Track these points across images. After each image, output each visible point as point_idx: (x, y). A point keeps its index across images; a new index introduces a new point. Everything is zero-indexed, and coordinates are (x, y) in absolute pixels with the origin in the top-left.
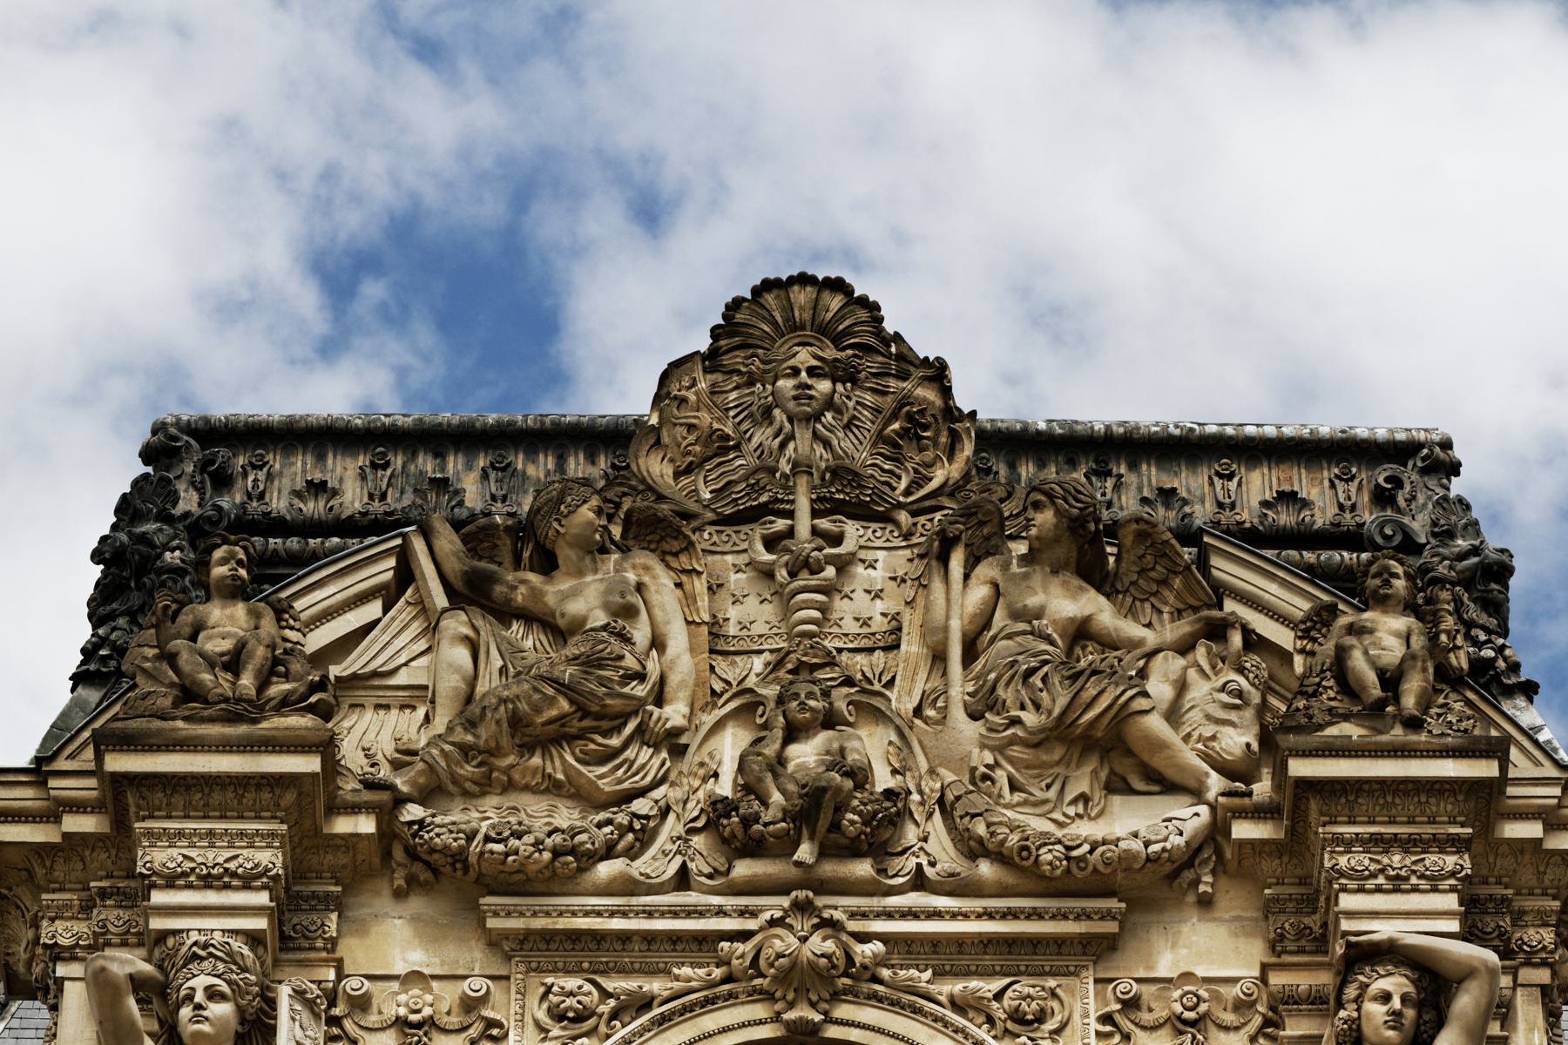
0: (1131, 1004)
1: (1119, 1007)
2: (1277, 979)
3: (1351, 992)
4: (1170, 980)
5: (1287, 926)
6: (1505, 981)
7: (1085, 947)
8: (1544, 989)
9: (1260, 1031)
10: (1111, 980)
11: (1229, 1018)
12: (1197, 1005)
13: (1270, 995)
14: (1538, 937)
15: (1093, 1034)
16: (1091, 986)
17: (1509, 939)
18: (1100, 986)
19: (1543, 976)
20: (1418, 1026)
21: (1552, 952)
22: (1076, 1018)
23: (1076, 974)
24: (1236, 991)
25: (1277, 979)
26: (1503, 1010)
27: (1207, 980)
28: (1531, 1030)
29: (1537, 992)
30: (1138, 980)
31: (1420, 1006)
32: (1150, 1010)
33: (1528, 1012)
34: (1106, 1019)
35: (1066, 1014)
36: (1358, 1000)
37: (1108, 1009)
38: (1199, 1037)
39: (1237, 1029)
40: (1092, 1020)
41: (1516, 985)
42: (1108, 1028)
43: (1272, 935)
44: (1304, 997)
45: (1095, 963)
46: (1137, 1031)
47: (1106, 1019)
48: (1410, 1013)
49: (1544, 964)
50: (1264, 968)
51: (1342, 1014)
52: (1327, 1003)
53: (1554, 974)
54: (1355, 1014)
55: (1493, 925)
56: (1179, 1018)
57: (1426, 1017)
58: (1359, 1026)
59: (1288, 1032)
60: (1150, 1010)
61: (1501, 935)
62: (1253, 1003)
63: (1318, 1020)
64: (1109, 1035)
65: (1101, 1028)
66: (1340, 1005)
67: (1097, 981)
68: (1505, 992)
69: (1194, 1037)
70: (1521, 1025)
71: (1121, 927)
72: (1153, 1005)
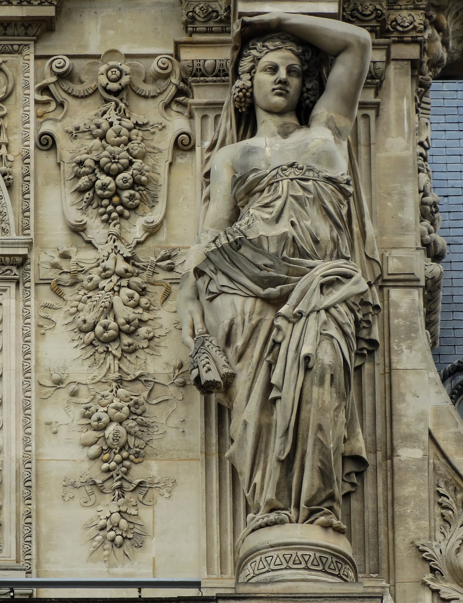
0: (65, 76)
1: (54, 79)
2: (188, 55)
3: (246, 64)
4: (98, 57)
5: (197, 10)
6: (380, 56)
7: (26, 28)
8: (415, 65)
9: (173, 100)
10: (48, 57)
11: (148, 89)
12: (120, 77)
13: (183, 69)
14: (410, 18)
15: (32, 103)
16: (32, 62)
17: (384, 20)
18: (39, 62)
19: (413, 52)
20: (302, 93)
21: (420, 32)
22: (19, 89)
23: (19, 52)
24: (153, 66)
25: (188, 55)
26: (376, 80)
27: (128, 56)
28: (402, 98)
29: (408, 66)
30: (70, 57)
31: (304, 76)
32: (82, 82)
33: (399, 84)
34: (44, 89)
35: (10, 86)
36: (252, 71)
37: (45, 82)
38: (122, 105)
39: (154, 97)
40: (32, 91)
41: (388, 61)
42: (45, 98)
43: (184, 18)
44: (210, 70)
45: (36, 42)
46: (70, 100)
47: (44, 89)
48: (295, 82)
49: (414, 41)
50: (177, 45)
51: (238, 83)
52: (227, 75)
53: (423, 51)
54: (249, 84)
55: (371, 8)
56: (105, 89)
57: (309, 86)
58: (252, 93)
59: (196, 100)
60: (82, 82)
61: (378, 17)
62: (167, 77)
63: (222, 90)
64: (46, 103)
65: (39, 98)
66: (236, 76)
67: (37, 58)
68: (379, 65)
69: (117, 105)
70: (393, 94)
71: (56, 12)
72: (83, 78)
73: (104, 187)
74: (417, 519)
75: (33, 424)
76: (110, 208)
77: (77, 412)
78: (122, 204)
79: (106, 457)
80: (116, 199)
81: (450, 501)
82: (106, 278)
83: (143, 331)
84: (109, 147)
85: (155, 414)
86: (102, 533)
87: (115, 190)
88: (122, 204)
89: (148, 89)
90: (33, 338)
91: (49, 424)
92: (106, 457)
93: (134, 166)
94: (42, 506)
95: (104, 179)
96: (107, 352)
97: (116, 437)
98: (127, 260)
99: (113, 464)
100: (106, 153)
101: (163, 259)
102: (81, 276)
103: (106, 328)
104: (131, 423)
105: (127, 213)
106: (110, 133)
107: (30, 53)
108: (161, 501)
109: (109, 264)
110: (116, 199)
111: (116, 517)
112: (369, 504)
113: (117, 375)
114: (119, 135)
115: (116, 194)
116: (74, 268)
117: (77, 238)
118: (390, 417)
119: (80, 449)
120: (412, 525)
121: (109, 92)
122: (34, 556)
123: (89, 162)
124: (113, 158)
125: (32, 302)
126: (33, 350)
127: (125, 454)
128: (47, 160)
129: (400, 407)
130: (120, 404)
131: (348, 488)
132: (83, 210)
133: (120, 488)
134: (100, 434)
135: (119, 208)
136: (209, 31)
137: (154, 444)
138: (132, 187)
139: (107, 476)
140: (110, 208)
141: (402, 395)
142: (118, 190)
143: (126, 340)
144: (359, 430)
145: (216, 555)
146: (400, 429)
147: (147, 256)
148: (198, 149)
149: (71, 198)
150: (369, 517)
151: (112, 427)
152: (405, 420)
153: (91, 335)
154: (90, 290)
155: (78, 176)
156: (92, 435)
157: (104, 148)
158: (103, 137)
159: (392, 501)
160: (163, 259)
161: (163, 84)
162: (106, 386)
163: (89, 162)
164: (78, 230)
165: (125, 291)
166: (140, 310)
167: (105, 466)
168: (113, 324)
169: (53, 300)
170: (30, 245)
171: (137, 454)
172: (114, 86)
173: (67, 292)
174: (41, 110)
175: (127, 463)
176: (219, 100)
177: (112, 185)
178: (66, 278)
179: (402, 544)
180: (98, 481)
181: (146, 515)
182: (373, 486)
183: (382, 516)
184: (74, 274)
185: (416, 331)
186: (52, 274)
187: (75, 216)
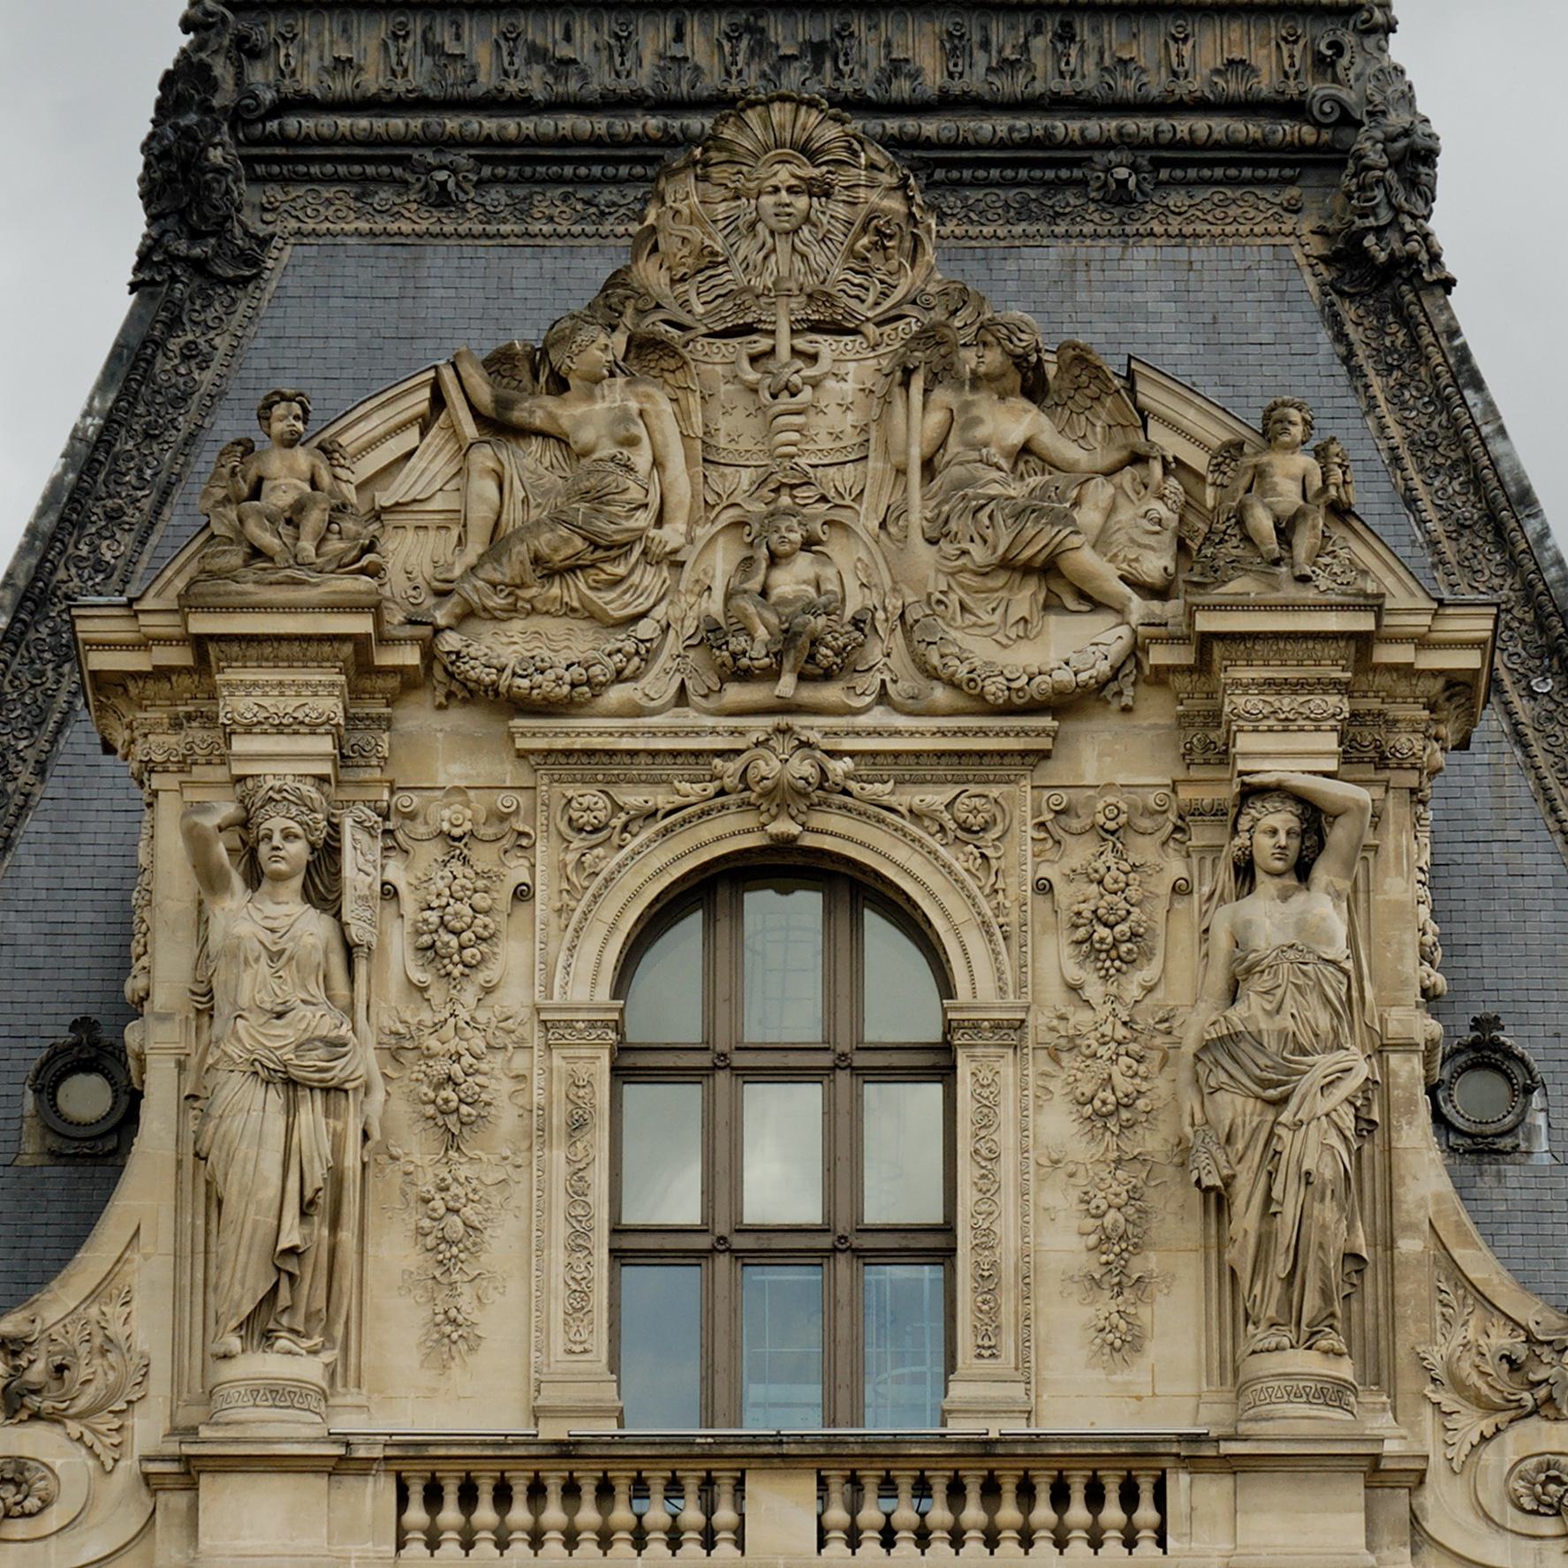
1: (1051, 816)
2: (1185, 794)
40: (1029, 828)
42: (1043, 835)
43: (1182, 750)
46: (1067, 837)
47: (1041, 825)
59: (1193, 842)
73: (1102, 941)
74: (1418, 1321)
75: (1032, 1212)
76: (1108, 963)
77: (1075, 1195)
78: (1119, 958)
79: (1104, 1248)
80: (1113, 954)
81: (1450, 1299)
82: (1105, 1044)
83: (1141, 1104)
84: (1108, 897)
85: (1153, 1198)
86: (1102, 1335)
87: (1112, 945)
88: (1119, 958)
89: (1146, 823)
90: (1030, 1112)
91: (1046, 1209)
92: (1104, 1248)
93: (1132, 917)
94: (1041, 1303)
95: (1102, 932)
96: (1105, 1126)
97: (1115, 1227)
98: (1125, 1024)
99: (1112, 1257)
100: (1103, 903)
101: (1161, 1021)
102: (1078, 1041)
103: (1104, 1103)
104: (1130, 1210)
105: (1124, 967)
106: (1108, 880)
107: (1026, 784)
108: (1159, 1298)
109: (1107, 1029)
110: (1113, 954)
111: (1115, 1318)
112: (1369, 1306)
113: (1116, 1154)
114: (1116, 882)
115: (1115, 946)
116: (1071, 1032)
117: (1073, 995)
118: (1390, 1201)
119: (1076, 1238)
120: (1412, 1328)
121: (1107, 831)
122: (1033, 1364)
123: (1087, 914)
124: (1111, 909)
125: (1030, 1072)
126: (1031, 1127)
127: (1124, 1245)
128: (1043, 904)
129: (1399, 1191)
130: (1118, 1190)
132: (1081, 965)
133: (1119, 1283)
134: (1099, 1222)
135: (1117, 963)
136: (1207, 763)
137: (1153, 1233)
138: (1129, 940)
139: (1104, 1269)
140: (1108, 963)
141: (1402, 1177)
142: (1116, 944)
143: (1125, 1115)
145: (1216, 1364)
146: (1400, 1217)
147: (1145, 1020)
148: (1196, 896)
149: (1068, 950)
150: (1369, 1321)
151: (1112, 1213)
152: (1405, 1207)
153: (1088, 1110)
154: (1088, 1057)
155: (1076, 926)
156: (1091, 1223)
157: (1102, 896)
158: (1100, 882)
159: (1392, 1300)
160: (1161, 1021)
161: (1160, 819)
162: (1102, 1166)
163: (1087, 914)
164: (1074, 989)
165: (1124, 1060)
166: (1137, 1081)
167: (1104, 1258)
168: (1112, 1099)
169: (1049, 1067)
170: (1028, 1008)
172: (1111, 825)
173: (1064, 1057)
174: (1039, 847)
175: (1126, 1255)
176: (1218, 842)
177: (1110, 940)
178: (1063, 1042)
179: (1402, 1352)
180: (1097, 1276)
181: (1145, 1313)
182: (1372, 1285)
183: (1382, 1320)
184: (1071, 1039)
185: (1416, 1104)
186: (1050, 1038)
187: (1074, 973)
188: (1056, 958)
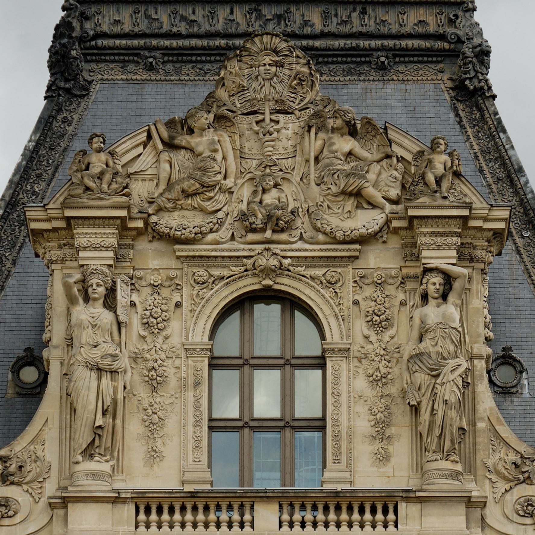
1: (359, 278)
22: (346, 281)
40: (351, 282)
42: (356, 285)
46: (364, 285)
47: (355, 282)
73: (376, 321)
76: (378, 329)
77: (367, 408)
78: (382, 327)
79: (377, 426)
80: (380, 325)
82: (377, 356)
83: (389, 377)
84: (378, 306)
86: (376, 455)
87: (379, 323)
88: (382, 327)
91: (357, 413)
92: (377, 426)
93: (386, 313)
94: (355, 445)
95: (376, 318)
96: (377, 384)
97: (380, 419)
98: (384, 349)
99: (379, 429)
100: (376, 308)
102: (368, 355)
103: (377, 376)
106: (378, 300)
107: (350, 267)
108: (396, 443)
109: (378, 351)
110: (380, 325)
111: (380, 450)
112: (467, 446)
113: (381, 394)
114: (381, 301)
115: (380, 323)
116: (366, 352)
117: (366, 339)
119: (367, 422)
121: (378, 284)
124: (379, 310)
127: (383, 425)
130: (382, 406)
131: (460, 440)
132: (369, 329)
133: (382, 438)
134: (375, 417)
135: (381, 329)
137: (393, 421)
138: (385, 321)
139: (377, 433)
140: (378, 329)
142: (381, 322)
143: (384, 380)
144: (464, 418)
145: (415, 465)
147: (391, 348)
149: (364, 324)
150: (467, 451)
151: (379, 414)
153: (371, 379)
154: (371, 361)
155: (367, 316)
156: (372, 417)
157: (376, 306)
158: (375, 301)
162: (376, 398)
163: (371, 312)
164: (366, 337)
165: (384, 362)
167: (377, 429)
168: (379, 375)
169: (358, 364)
171: (387, 425)
172: (379, 282)
173: (363, 361)
175: (384, 428)
177: (379, 321)
178: (363, 355)
180: (374, 436)
181: (391, 448)
182: (468, 439)
183: (471, 450)
184: (365, 354)
186: (358, 354)
187: (366, 332)
188: (360, 327)
